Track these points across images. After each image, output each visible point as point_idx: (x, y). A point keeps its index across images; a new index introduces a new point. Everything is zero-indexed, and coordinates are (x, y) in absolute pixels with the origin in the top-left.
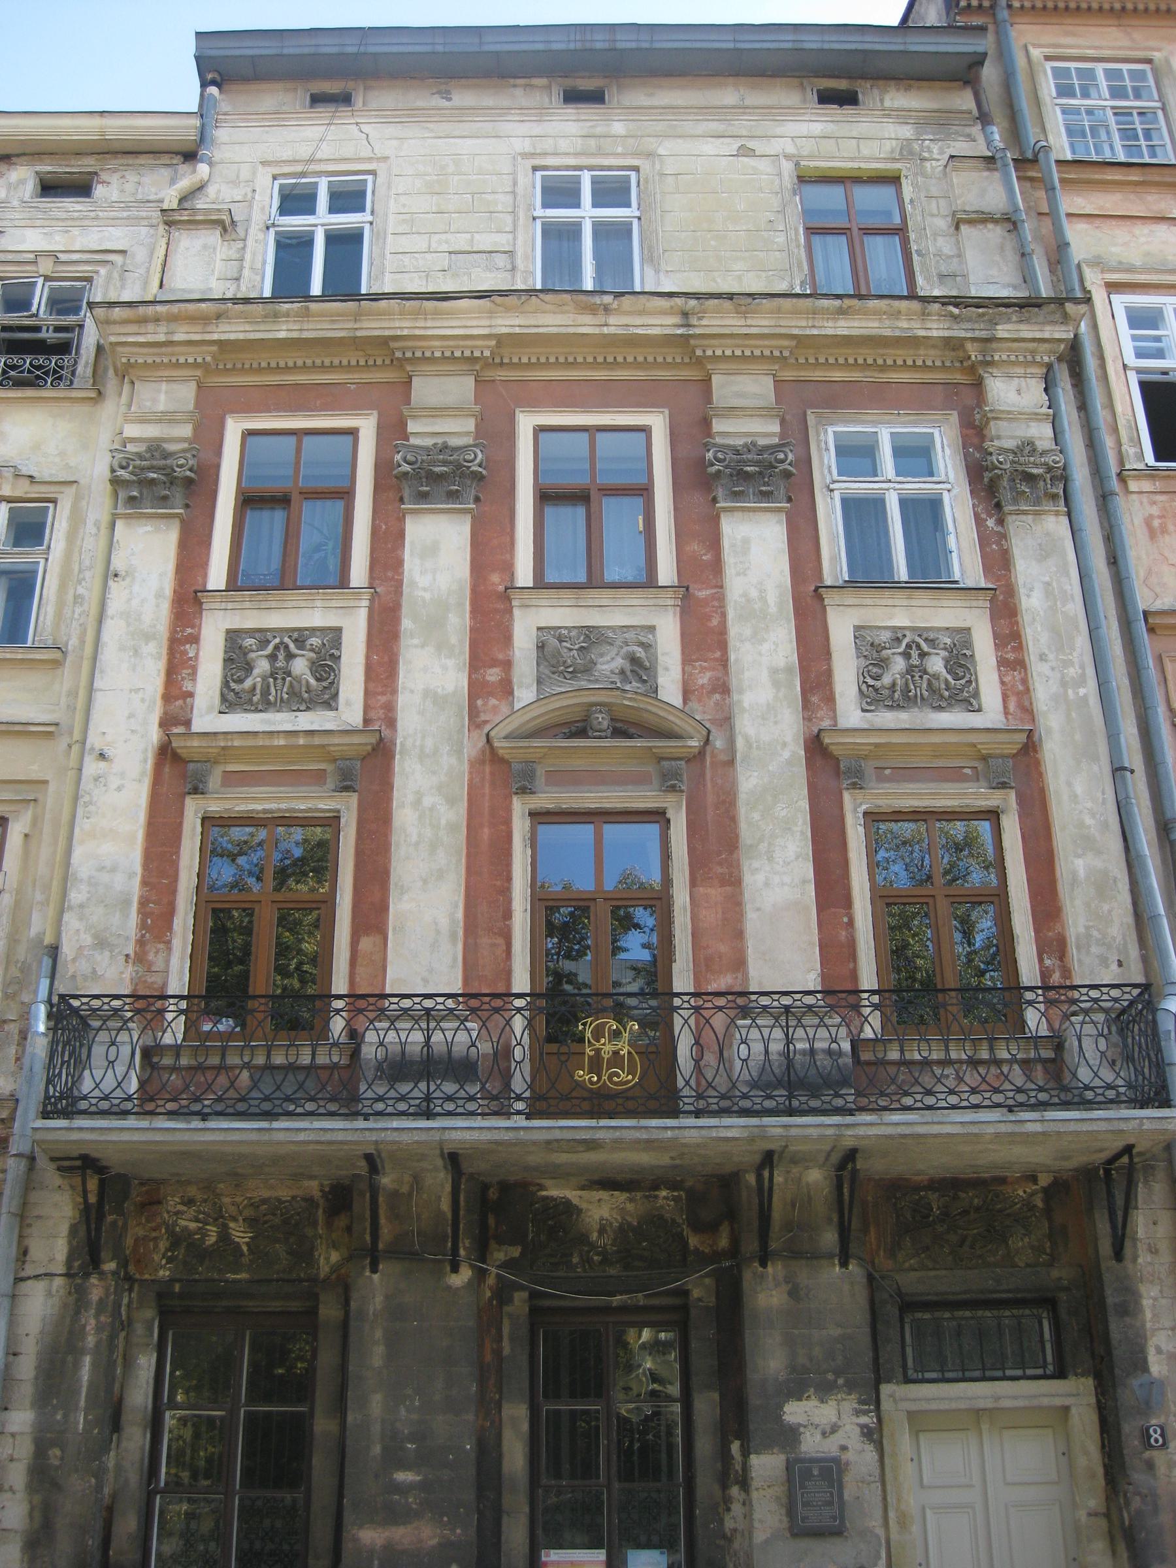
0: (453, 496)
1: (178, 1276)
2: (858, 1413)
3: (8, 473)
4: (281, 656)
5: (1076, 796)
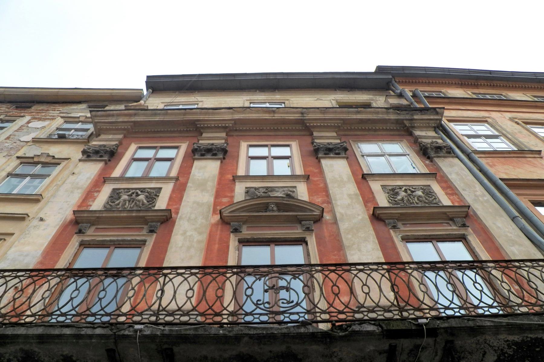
0: (215, 155)
3: (45, 155)
4: (134, 195)
5: (499, 227)
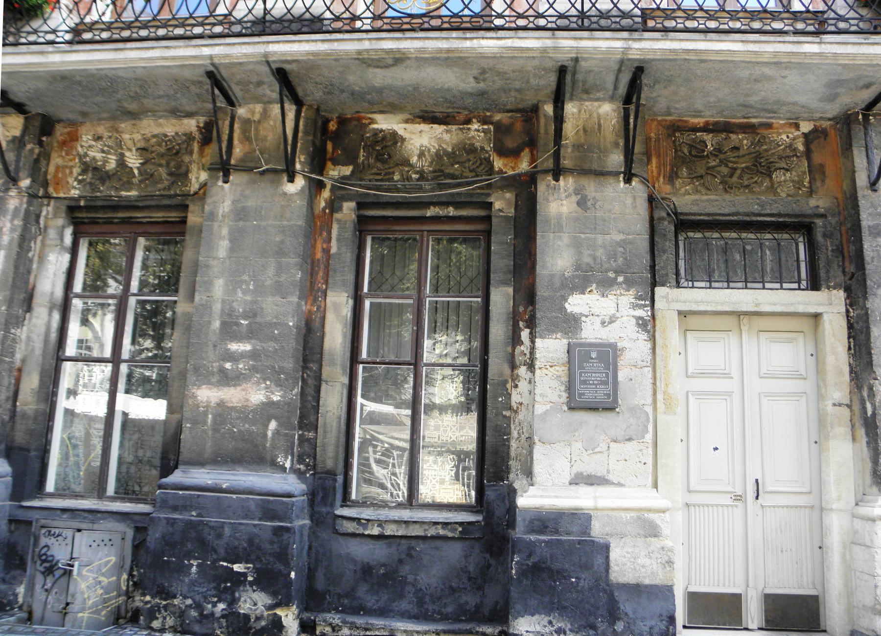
1: (85, 194)
2: (635, 306)
